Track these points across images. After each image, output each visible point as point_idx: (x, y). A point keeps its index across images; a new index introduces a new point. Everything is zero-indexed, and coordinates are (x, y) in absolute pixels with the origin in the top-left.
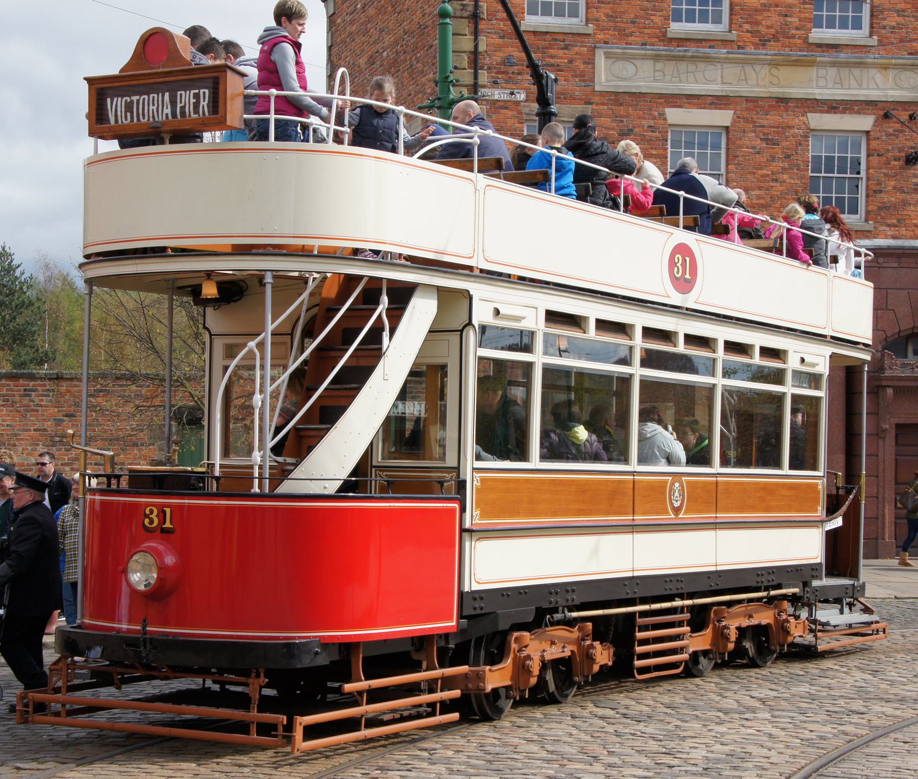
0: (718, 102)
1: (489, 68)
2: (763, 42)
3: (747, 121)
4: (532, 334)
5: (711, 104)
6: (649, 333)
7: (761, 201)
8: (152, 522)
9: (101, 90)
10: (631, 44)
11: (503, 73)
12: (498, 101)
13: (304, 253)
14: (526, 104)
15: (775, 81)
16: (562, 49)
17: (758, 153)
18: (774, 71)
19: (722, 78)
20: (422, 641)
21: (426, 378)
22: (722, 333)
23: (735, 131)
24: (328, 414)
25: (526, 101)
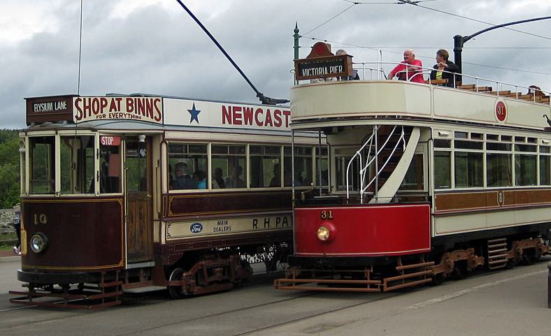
4: (450, 141)
6: (489, 137)
8: (324, 216)
9: (300, 66)
13: (373, 118)
20: (419, 254)
21: (418, 160)
22: (514, 134)
24: (385, 176)
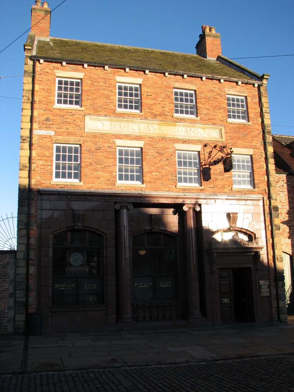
0: (138, 138)
1: (39, 122)
2: (155, 116)
3: (150, 145)
5: (134, 138)
14: (55, 136)
15: (161, 131)
16: (70, 116)
18: (160, 128)
23: (145, 149)
25: (55, 135)
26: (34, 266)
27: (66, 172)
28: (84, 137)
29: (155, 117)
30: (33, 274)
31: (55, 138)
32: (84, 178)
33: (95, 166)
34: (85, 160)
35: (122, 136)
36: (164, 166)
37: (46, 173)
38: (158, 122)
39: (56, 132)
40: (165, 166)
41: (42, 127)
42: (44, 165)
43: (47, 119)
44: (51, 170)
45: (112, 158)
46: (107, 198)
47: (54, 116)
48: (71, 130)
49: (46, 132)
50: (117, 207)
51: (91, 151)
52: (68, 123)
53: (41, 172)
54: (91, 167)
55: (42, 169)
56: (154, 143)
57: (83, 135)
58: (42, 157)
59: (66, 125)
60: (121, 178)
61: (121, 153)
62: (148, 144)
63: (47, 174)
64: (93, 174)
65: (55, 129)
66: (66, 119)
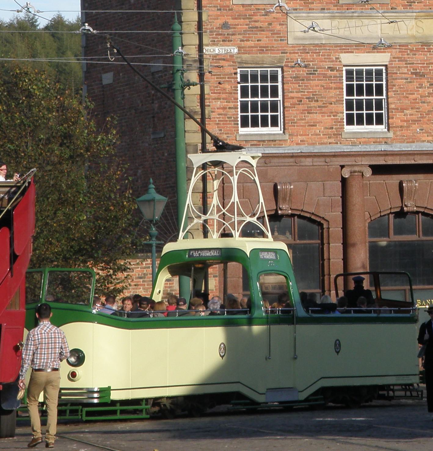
7: (414, 117)
10: (313, 9)
11: (221, 34)
12: (218, 55)
14: (239, 55)
15: (421, 31)
16: (263, 15)
17: (410, 82)
18: (419, 23)
19: (381, 30)
23: (393, 67)
25: (239, 53)
26: (214, 277)
27: (258, 115)
28: (288, 54)
29: (411, 5)
30: (214, 290)
31: (240, 58)
32: (290, 126)
33: (307, 104)
34: (290, 95)
35: (352, 46)
36: (426, 97)
37: (227, 121)
38: (415, 14)
39: (240, 48)
40: (428, 96)
41: (216, 40)
42: (224, 108)
43: (225, 26)
44: (235, 116)
45: (335, 89)
46: (328, 160)
47: (236, 19)
48: (265, 41)
49: (223, 50)
50: (346, 174)
51: (299, 77)
52: (259, 29)
53: (219, 121)
54: (301, 107)
55: (221, 114)
56: (408, 54)
57: (285, 50)
58: (220, 93)
59: (257, 34)
60: (350, 122)
61: (349, 73)
62: (398, 58)
63: (229, 124)
64: (305, 119)
65: (239, 42)
66: (256, 21)
